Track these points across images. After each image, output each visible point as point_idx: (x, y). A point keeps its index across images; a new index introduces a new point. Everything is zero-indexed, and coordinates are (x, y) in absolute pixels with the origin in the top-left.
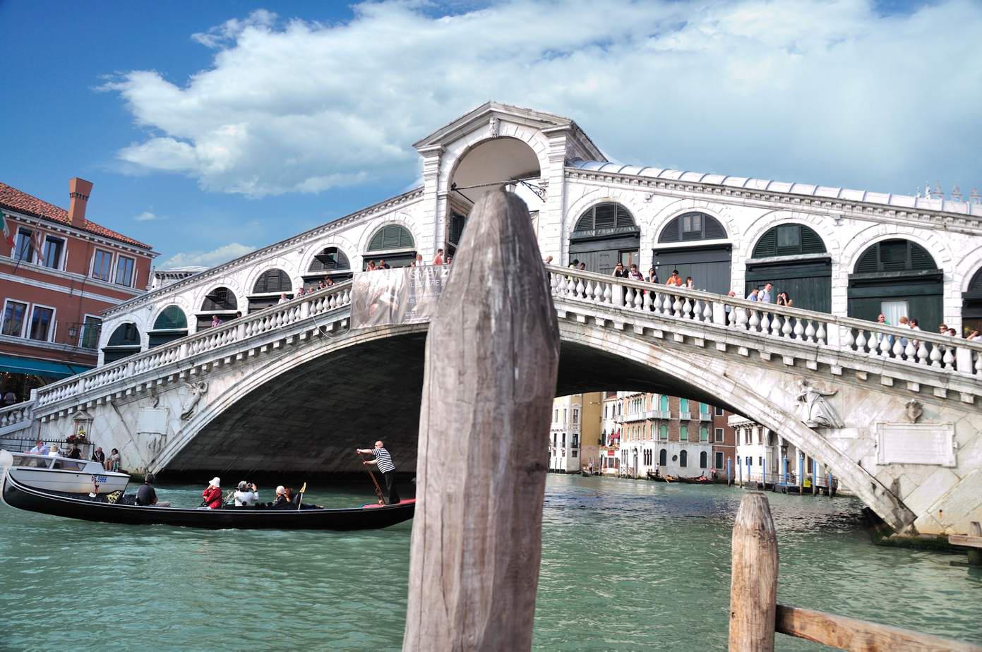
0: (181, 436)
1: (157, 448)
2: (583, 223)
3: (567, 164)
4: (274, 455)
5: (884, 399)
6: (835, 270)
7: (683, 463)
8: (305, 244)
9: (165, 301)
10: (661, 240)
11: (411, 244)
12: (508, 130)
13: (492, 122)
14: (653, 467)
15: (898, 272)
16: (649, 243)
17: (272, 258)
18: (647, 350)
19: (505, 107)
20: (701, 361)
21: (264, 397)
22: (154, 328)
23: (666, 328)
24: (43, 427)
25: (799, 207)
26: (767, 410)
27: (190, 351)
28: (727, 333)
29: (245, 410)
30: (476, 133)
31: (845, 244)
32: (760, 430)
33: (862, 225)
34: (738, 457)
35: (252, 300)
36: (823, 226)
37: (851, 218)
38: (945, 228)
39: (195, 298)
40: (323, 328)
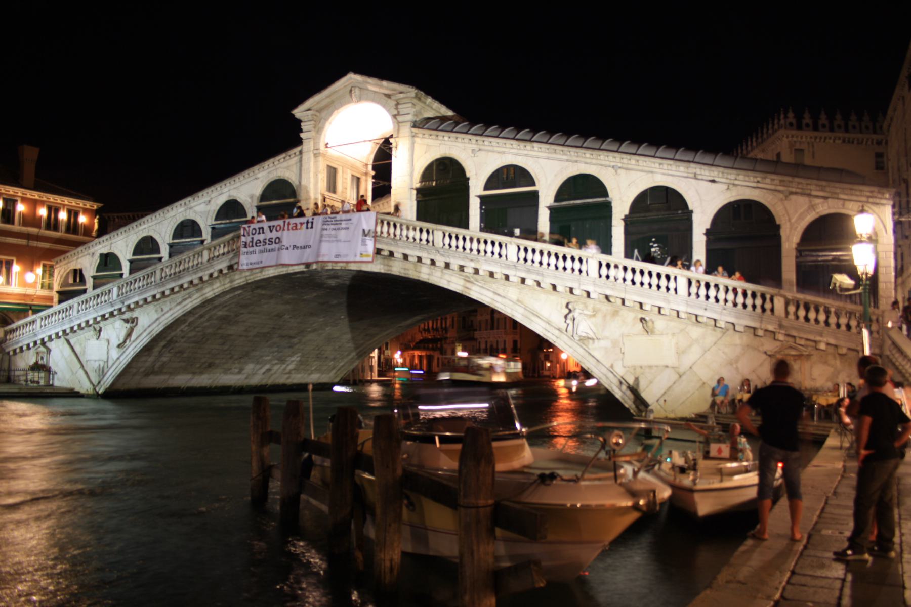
0: (118, 362)
1: (102, 372)
2: (427, 173)
4: (201, 373)
10: (486, 188)
18: (462, 282)
21: (183, 327)
22: (97, 271)
23: (473, 265)
24: (13, 358)
25: (589, 161)
26: (548, 327)
29: (168, 338)
33: (634, 175)
35: (171, 246)
37: (626, 169)
38: (695, 177)
39: (127, 246)
40: (221, 271)
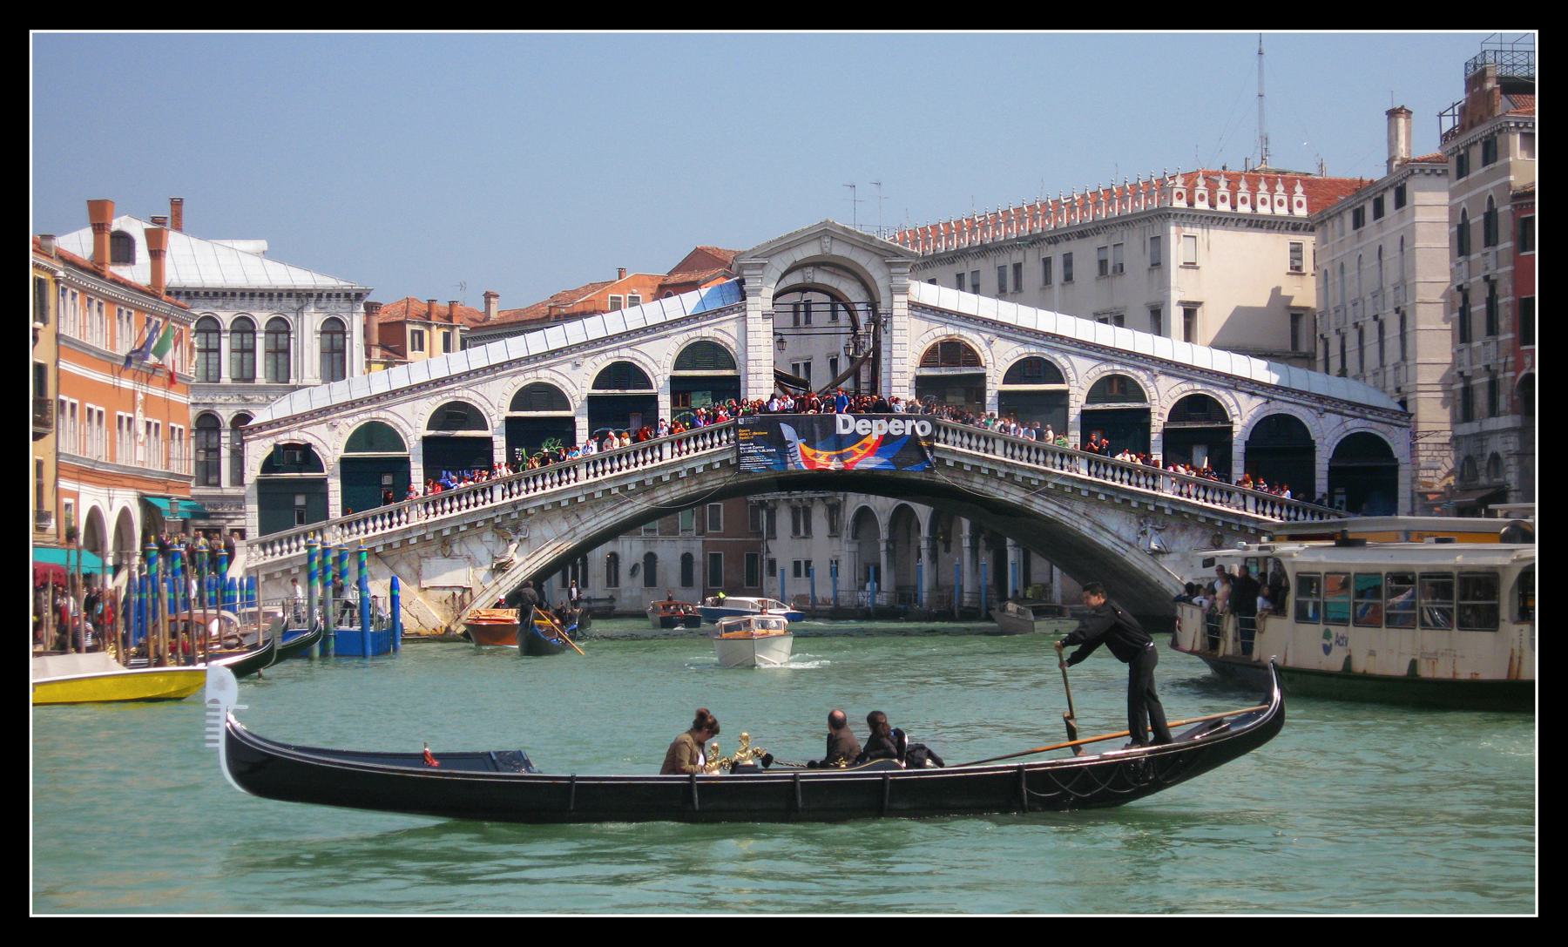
2: (926, 361)
7: (650, 580)
8: (585, 356)
9: (363, 416)
10: (1006, 381)
11: (734, 367)
12: (839, 251)
14: (598, 588)
15: (1199, 422)
17: (536, 369)
19: (845, 229)
30: (803, 248)
32: (834, 511)
34: (772, 563)
36: (1141, 377)
38: (1236, 389)
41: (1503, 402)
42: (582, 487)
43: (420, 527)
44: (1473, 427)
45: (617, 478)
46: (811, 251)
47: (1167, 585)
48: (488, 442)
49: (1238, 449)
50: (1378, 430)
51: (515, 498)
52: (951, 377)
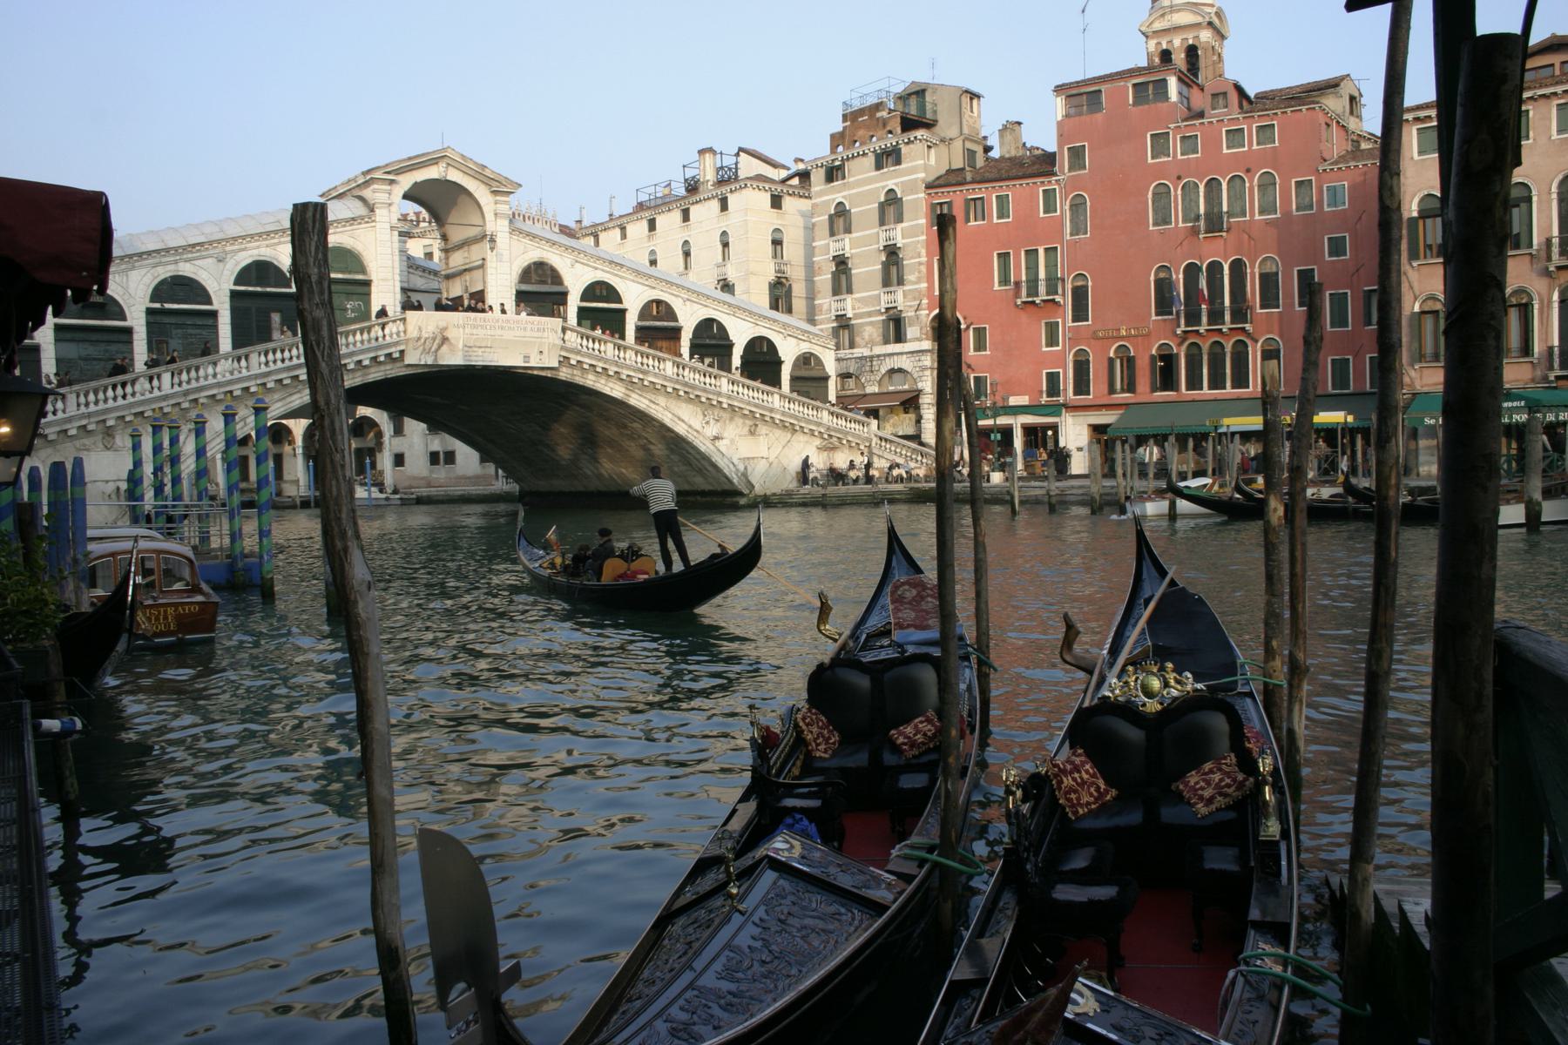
3: (511, 222)
5: (739, 421)
6: (683, 333)
12: (454, 176)
13: (442, 165)
16: (574, 303)
17: (176, 262)
19: (463, 156)
20: (653, 397)
27: (176, 380)
28: (677, 382)
31: (688, 318)
36: (677, 305)
41: (911, 332)
42: (257, 376)
43: (83, 416)
44: (857, 352)
45: (289, 369)
46: (433, 173)
47: (721, 463)
48: (129, 331)
49: (736, 361)
50: (817, 350)
51: (185, 386)
52: (541, 292)
